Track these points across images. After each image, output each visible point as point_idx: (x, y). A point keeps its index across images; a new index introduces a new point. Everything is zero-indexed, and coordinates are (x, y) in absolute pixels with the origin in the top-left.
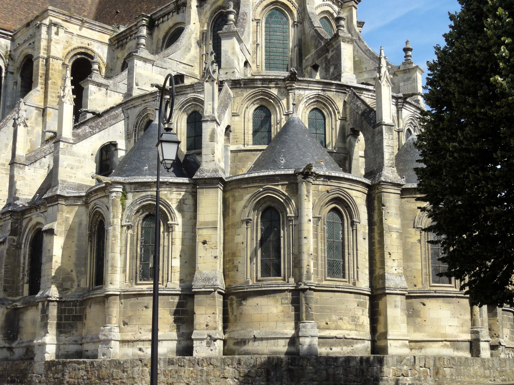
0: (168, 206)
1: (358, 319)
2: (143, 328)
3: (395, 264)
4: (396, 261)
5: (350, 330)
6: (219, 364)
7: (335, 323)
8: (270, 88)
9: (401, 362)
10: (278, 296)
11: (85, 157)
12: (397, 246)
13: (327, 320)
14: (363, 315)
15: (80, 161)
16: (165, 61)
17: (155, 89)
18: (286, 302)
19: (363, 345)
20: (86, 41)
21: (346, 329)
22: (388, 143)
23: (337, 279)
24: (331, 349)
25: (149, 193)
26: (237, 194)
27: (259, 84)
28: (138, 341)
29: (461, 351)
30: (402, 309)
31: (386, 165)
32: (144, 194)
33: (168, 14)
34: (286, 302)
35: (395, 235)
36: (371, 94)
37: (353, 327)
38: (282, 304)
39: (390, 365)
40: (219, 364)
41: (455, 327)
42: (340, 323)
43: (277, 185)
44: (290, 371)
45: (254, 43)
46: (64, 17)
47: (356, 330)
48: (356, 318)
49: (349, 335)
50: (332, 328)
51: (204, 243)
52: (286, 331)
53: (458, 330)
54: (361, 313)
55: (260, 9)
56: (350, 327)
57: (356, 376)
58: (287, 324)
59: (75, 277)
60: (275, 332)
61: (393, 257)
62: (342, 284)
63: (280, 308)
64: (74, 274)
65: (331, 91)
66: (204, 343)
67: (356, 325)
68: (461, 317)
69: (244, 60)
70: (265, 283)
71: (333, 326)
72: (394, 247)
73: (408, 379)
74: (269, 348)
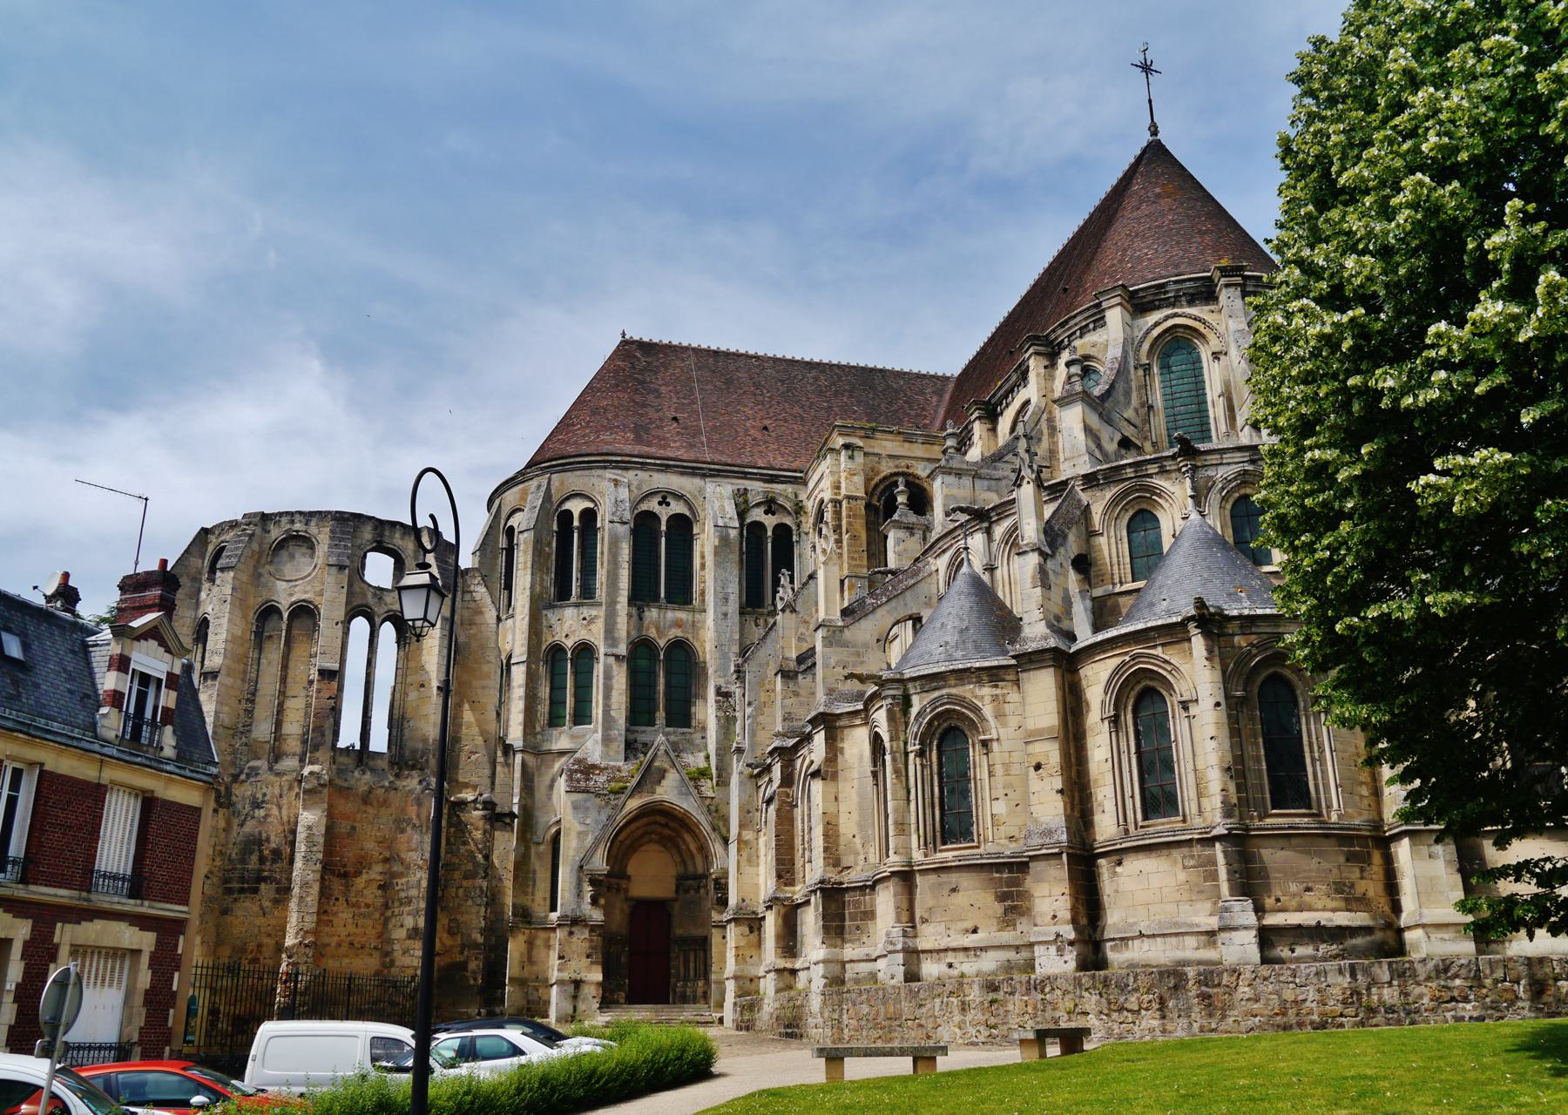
0: (976, 710)
1: (1352, 886)
2: (953, 926)
5: (1334, 910)
6: (1071, 988)
8: (1150, 476)
10: (1177, 854)
11: (866, 645)
13: (1279, 893)
14: (1362, 878)
15: (858, 654)
16: (995, 468)
17: (964, 517)
18: (1192, 863)
19: (1368, 938)
20: (903, 462)
21: (1324, 910)
25: (944, 691)
26: (1090, 673)
27: (1130, 472)
28: (946, 950)
30: (1448, 862)
32: (937, 694)
33: (1012, 391)
34: (1192, 863)
37: (1343, 904)
38: (1185, 867)
39: (1421, 978)
40: (1071, 988)
42: (1308, 897)
43: (1154, 647)
44: (1204, 997)
45: (1142, 405)
46: (862, 433)
51: (1038, 767)
52: (1196, 920)
54: (1358, 874)
55: (1146, 346)
56: (1334, 904)
57: (1344, 1002)
58: (1199, 905)
59: (859, 847)
60: (1176, 924)
63: (1182, 876)
64: (858, 840)
66: (1053, 949)
67: (1346, 900)
69: (1118, 437)
70: (1151, 830)
71: (1294, 903)
73: (1468, 1007)
74: (1168, 953)
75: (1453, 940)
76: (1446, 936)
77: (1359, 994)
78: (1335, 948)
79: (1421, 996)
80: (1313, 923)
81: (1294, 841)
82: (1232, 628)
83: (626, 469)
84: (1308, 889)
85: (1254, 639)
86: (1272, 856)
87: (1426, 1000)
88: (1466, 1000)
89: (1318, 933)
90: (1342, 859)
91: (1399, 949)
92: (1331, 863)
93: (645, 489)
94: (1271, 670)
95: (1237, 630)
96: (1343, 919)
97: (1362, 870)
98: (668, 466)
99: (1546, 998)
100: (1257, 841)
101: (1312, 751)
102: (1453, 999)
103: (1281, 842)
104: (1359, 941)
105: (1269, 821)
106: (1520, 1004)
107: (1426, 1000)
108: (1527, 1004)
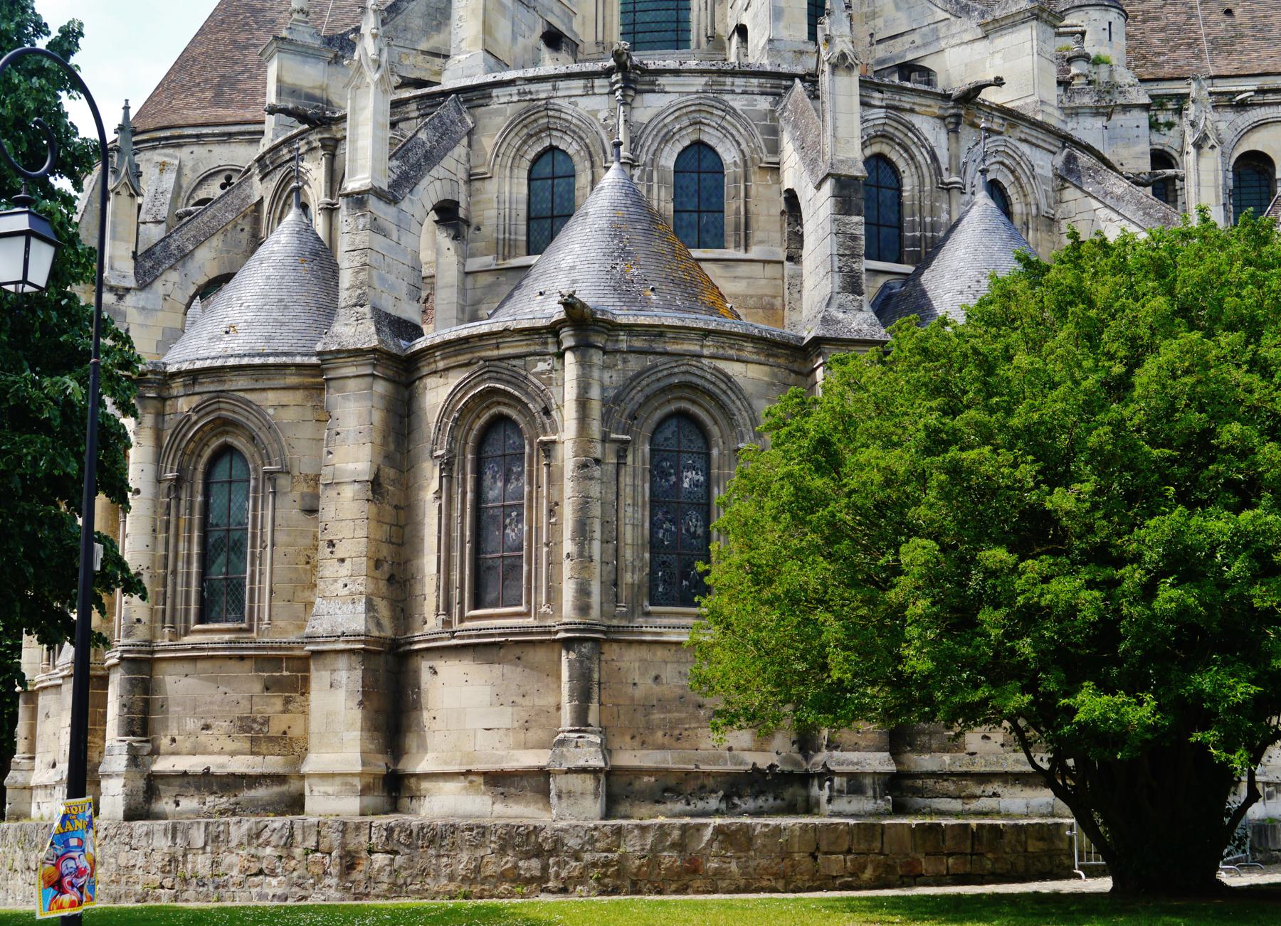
1: (266, 721)
3: (345, 570)
4: (348, 562)
7: (193, 739)
9: (258, 835)
12: (354, 520)
14: (285, 711)
21: (221, 752)
22: (353, 243)
23: (216, 626)
24: (178, 805)
29: (516, 802)
30: (350, 693)
31: (343, 305)
35: (348, 492)
36: (513, 90)
37: (247, 746)
41: (501, 732)
42: (204, 737)
47: (252, 753)
48: (254, 721)
49: (223, 766)
50: (184, 750)
53: (510, 740)
61: (340, 552)
62: (216, 637)
65: (408, 119)
67: (253, 740)
68: (526, 702)
71: (188, 744)
72: (344, 523)
73: (274, 882)
75: (337, 795)
76: (330, 790)
77: (177, 861)
78: (224, 802)
79: (231, 867)
80: (200, 770)
81: (200, 665)
82: (177, 387)
83: (179, 146)
84: (207, 727)
85: (195, 400)
86: (176, 685)
87: (235, 872)
88: (273, 873)
89: (206, 782)
90: (257, 688)
91: (296, 804)
92: (244, 688)
93: (203, 169)
94: (222, 440)
95: (182, 391)
96: (241, 764)
97: (287, 701)
98: (230, 135)
99: (355, 875)
100: (164, 665)
101: (253, 546)
102: (261, 872)
103: (187, 667)
104: (261, 793)
105: (187, 639)
106: (328, 881)
107: (235, 872)
108: (333, 881)
